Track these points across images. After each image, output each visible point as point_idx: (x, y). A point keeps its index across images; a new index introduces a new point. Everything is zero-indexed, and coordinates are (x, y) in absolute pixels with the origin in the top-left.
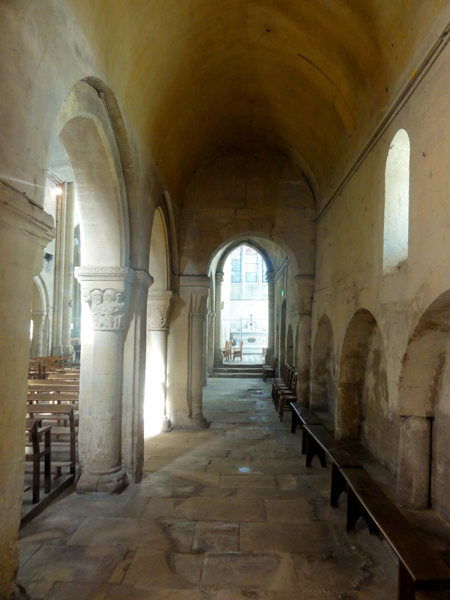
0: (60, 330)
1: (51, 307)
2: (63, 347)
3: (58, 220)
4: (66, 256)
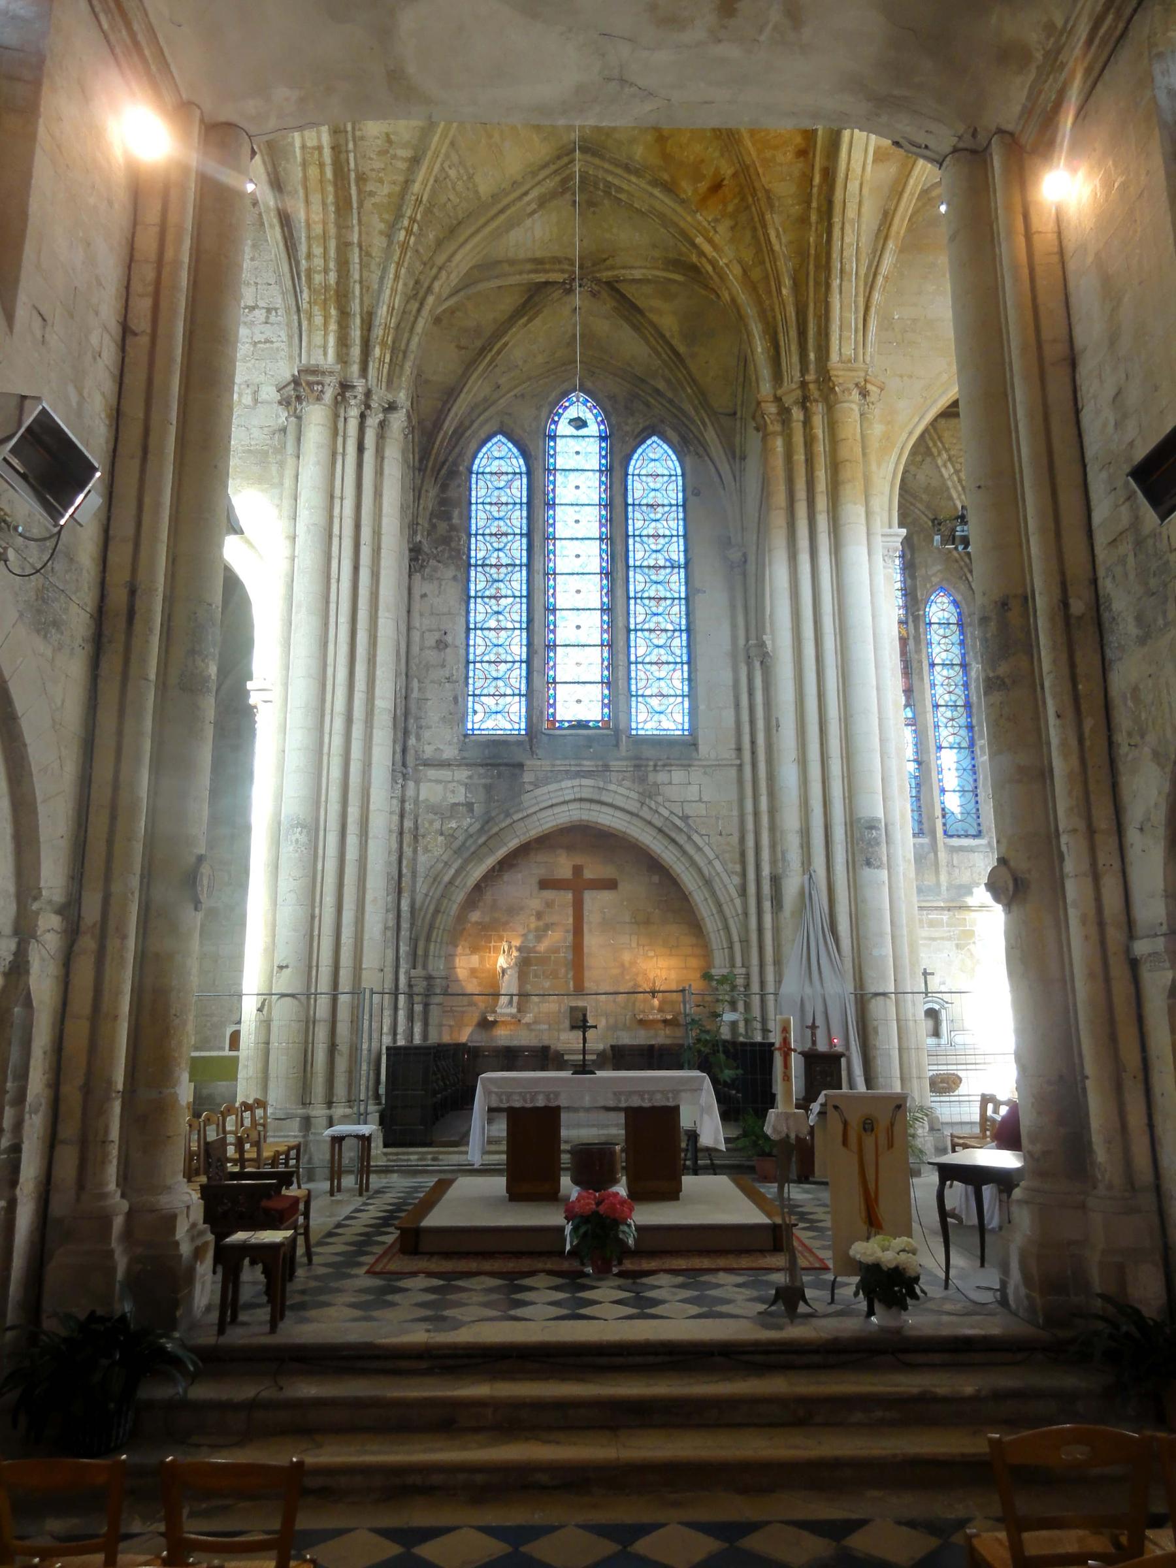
0: (110, 1083)
1: (50, 902)
2: (130, 1215)
3: (133, 325)
4: (173, 560)
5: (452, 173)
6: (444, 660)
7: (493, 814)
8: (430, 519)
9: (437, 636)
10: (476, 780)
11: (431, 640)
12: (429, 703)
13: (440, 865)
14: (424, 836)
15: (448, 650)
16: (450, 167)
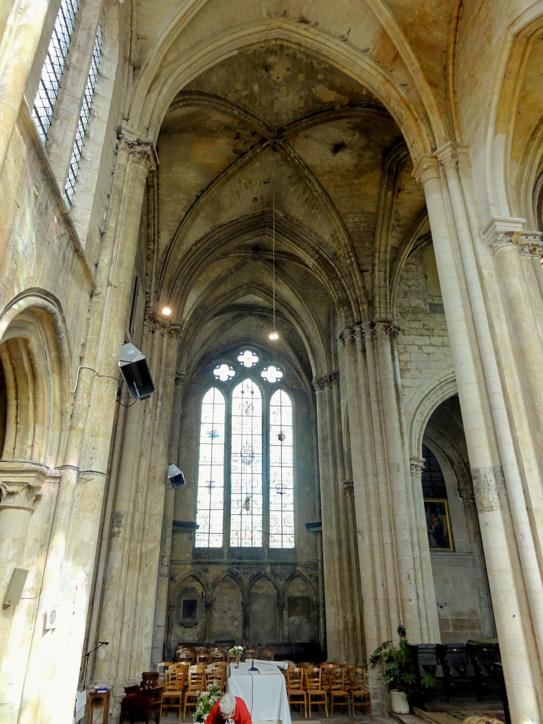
5: (356, 219)
16: (354, 219)
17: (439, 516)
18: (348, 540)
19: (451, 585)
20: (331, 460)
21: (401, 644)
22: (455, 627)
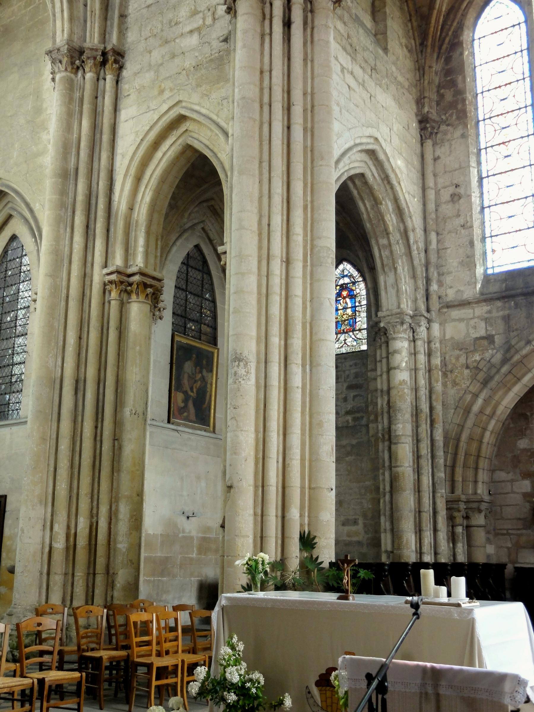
6: (459, 210)
7: (513, 342)
8: (438, 92)
9: (452, 190)
10: (495, 314)
11: (445, 195)
12: (449, 251)
13: (469, 397)
14: (451, 372)
15: (462, 201)
17: (205, 372)
18: (100, 382)
19: (203, 484)
20: (79, 220)
21: (302, 565)
22: (201, 550)
